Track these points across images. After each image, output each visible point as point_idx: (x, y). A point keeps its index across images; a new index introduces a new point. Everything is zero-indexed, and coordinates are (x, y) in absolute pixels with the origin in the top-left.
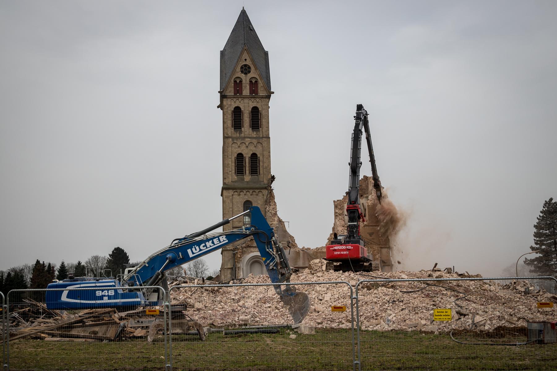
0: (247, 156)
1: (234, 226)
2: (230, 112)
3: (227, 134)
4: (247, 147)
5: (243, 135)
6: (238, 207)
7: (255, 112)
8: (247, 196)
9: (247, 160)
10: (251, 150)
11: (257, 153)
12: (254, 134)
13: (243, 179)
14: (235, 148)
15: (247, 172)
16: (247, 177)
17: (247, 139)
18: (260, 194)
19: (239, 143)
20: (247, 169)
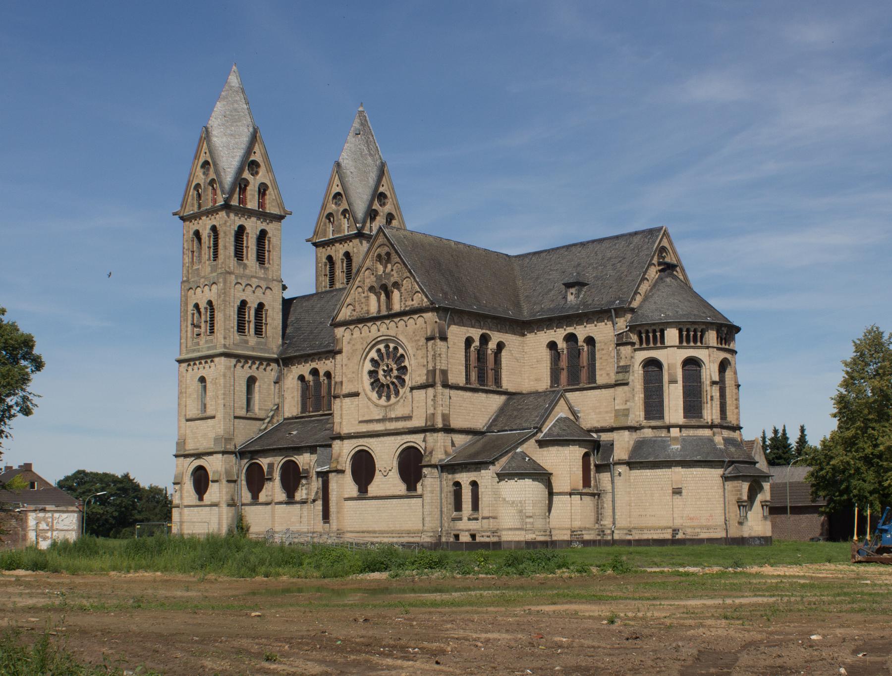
0: (253, 305)
1: (236, 415)
2: (233, 233)
3: (229, 268)
4: (254, 292)
5: (247, 272)
6: (240, 384)
7: (262, 236)
8: (253, 372)
9: (252, 312)
10: (257, 296)
11: (265, 303)
12: (261, 273)
13: (247, 342)
14: (239, 291)
15: (252, 331)
16: (252, 339)
17: (254, 280)
18: (269, 368)
19: (244, 285)
20: (252, 326)
